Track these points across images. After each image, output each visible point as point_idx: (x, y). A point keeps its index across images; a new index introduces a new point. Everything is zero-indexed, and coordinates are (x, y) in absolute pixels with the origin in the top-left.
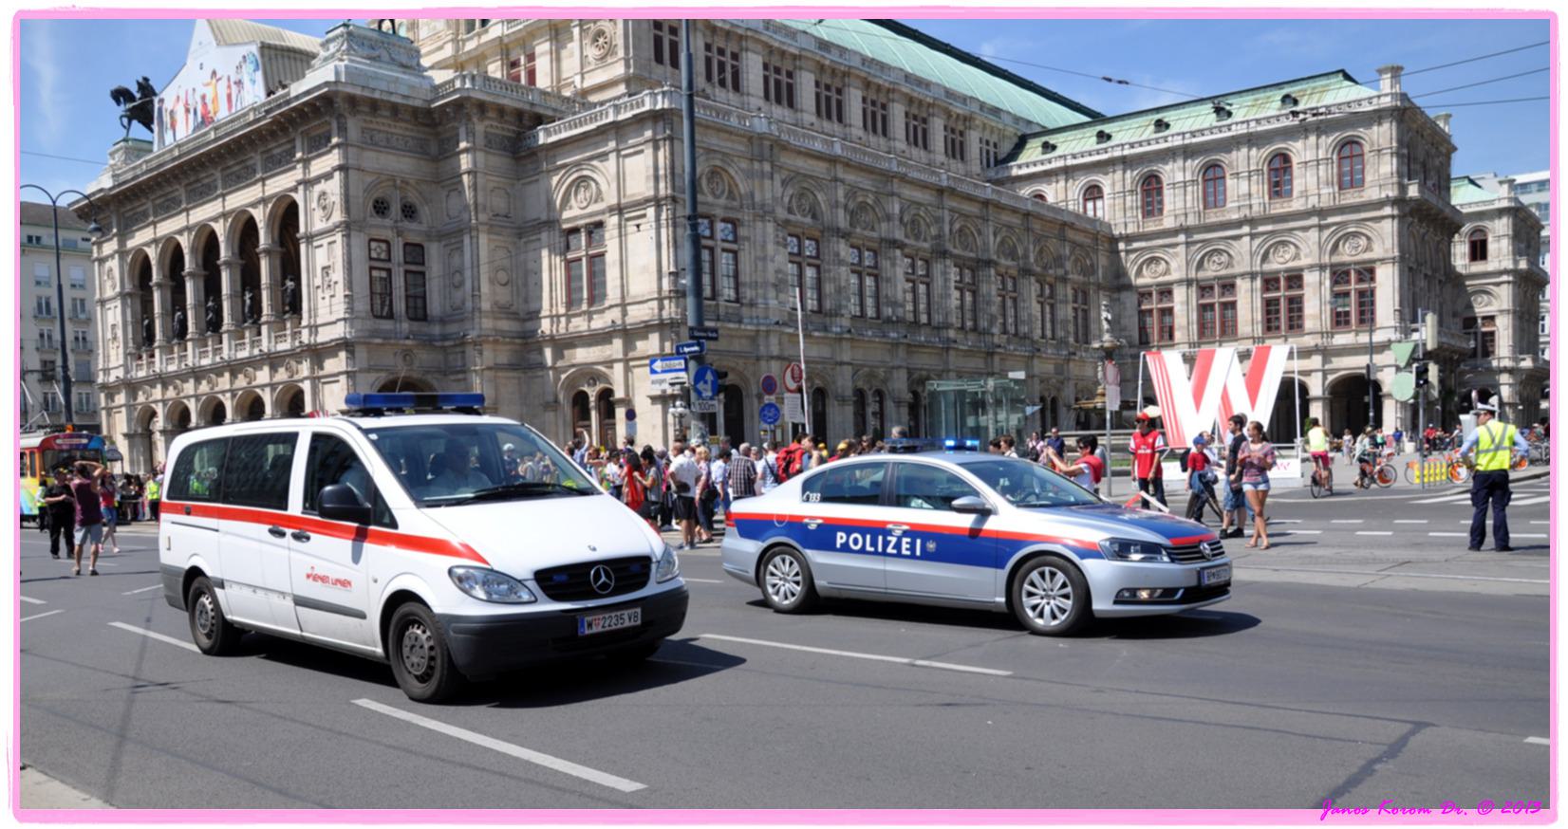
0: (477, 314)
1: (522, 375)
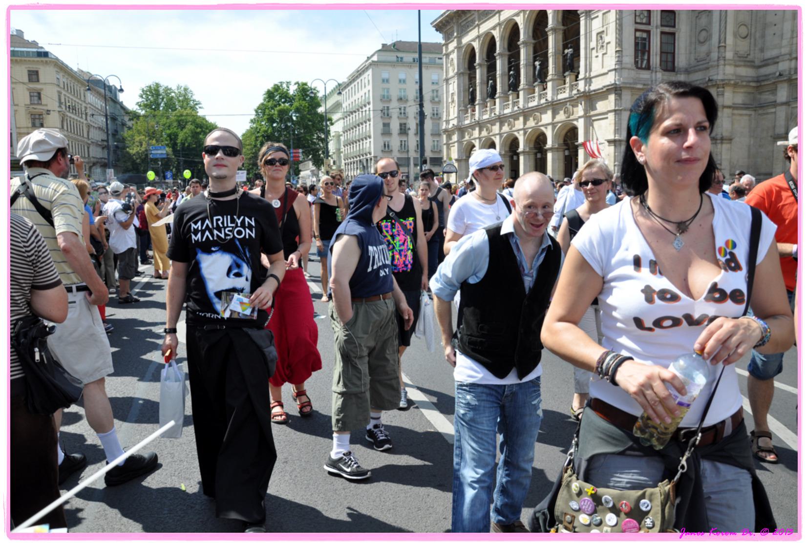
0: (722, 62)
1: (753, 113)
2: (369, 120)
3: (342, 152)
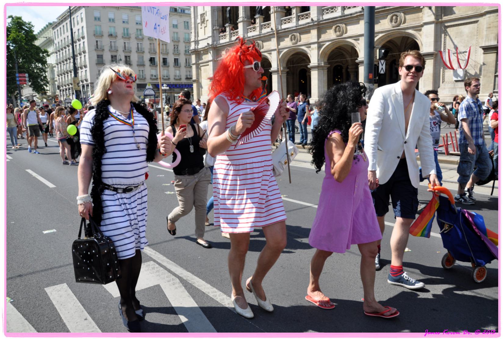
2: (84, 52)
3: (56, 81)
